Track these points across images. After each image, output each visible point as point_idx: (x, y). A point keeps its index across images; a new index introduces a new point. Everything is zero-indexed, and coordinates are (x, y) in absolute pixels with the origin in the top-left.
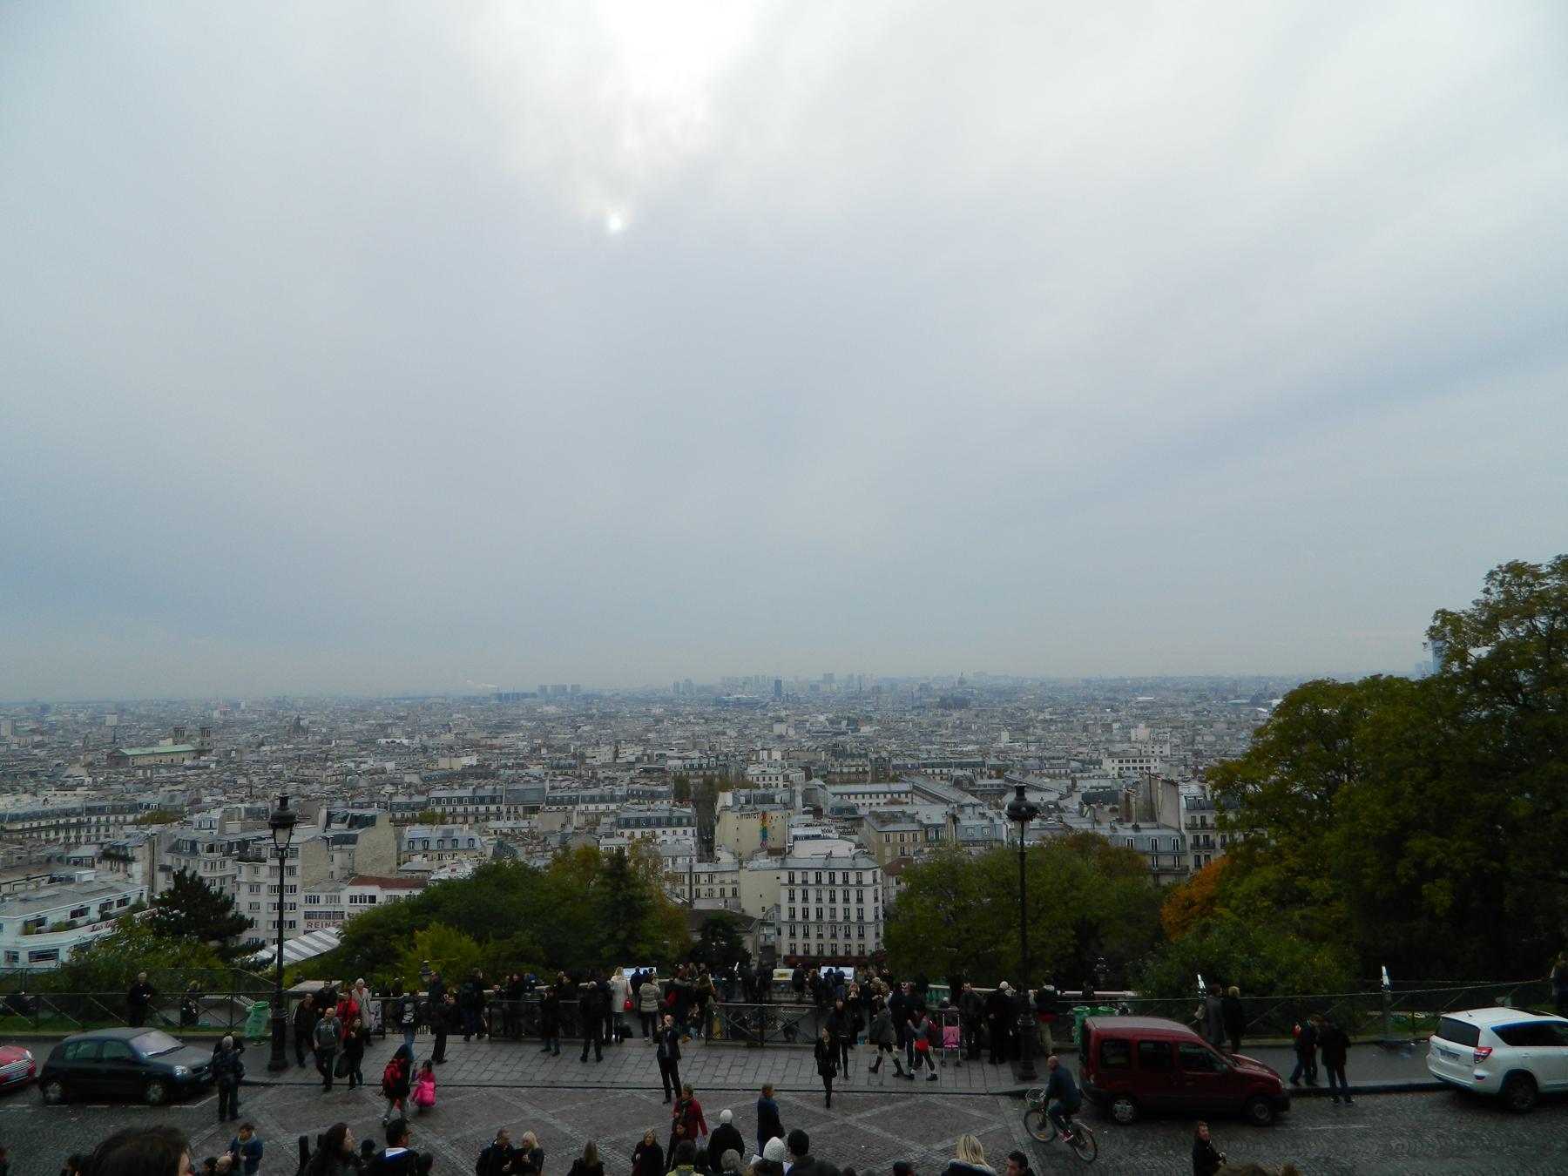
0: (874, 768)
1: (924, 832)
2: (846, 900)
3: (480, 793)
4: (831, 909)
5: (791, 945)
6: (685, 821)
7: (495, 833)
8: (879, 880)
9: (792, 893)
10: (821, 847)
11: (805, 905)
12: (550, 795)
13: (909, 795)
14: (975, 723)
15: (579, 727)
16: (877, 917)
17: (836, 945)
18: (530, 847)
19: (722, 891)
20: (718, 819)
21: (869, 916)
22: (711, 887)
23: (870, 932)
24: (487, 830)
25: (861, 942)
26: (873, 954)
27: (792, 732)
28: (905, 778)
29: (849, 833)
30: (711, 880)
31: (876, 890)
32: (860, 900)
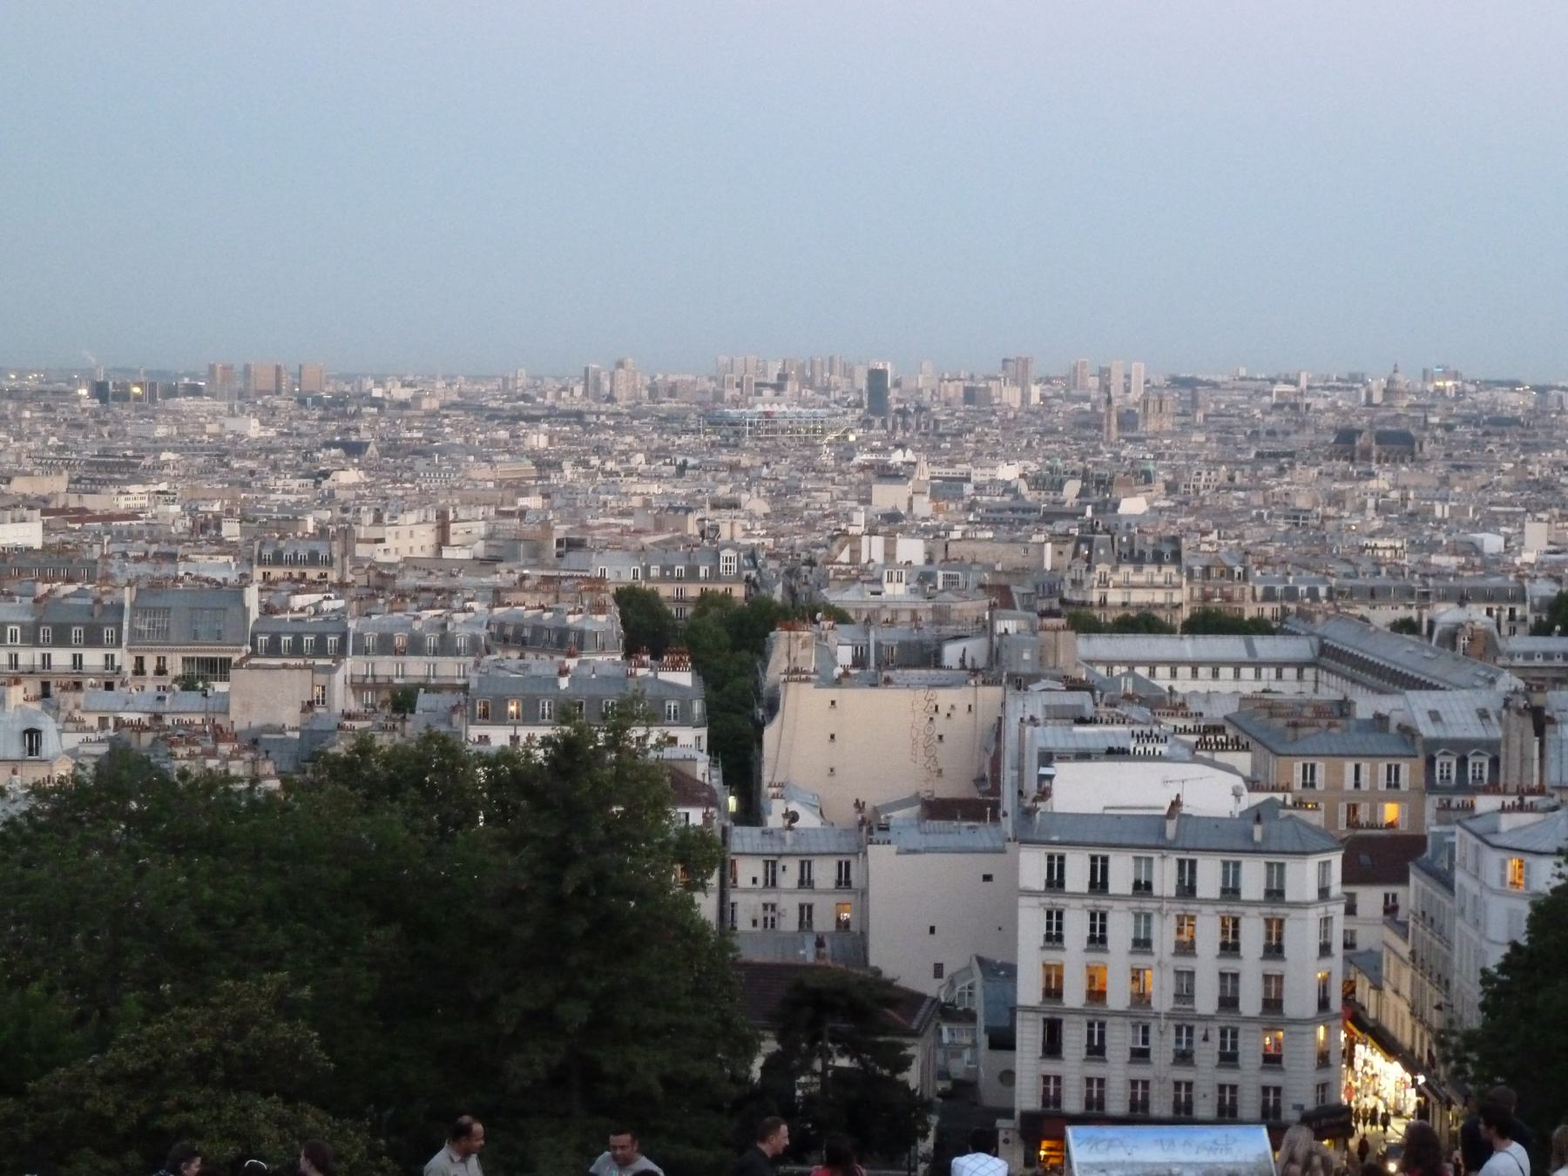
0: (1197, 593)
1: (1420, 762)
2: (1230, 948)
4: (1179, 973)
7: (103, 722)
9: (1055, 919)
12: (259, 628)
13: (1309, 673)
14: (1445, 500)
15: (326, 475)
17: (1189, 1085)
18: (212, 763)
19: (806, 912)
20: (773, 708)
22: (770, 898)
24: (77, 714)
25: (1271, 1079)
27: (923, 506)
29: (1223, 747)
30: (771, 882)
31: (1326, 921)
32: (1274, 950)
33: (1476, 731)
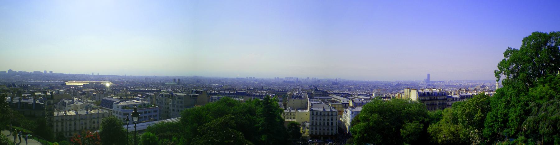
3: (231, 92)
5: (312, 132)
6: (280, 101)
8: (337, 115)
10: (321, 106)
11: (316, 121)
16: (336, 125)
21: (334, 124)
23: (334, 129)
26: (335, 134)
28: (330, 96)
30: (288, 115)
33: (347, 102)
